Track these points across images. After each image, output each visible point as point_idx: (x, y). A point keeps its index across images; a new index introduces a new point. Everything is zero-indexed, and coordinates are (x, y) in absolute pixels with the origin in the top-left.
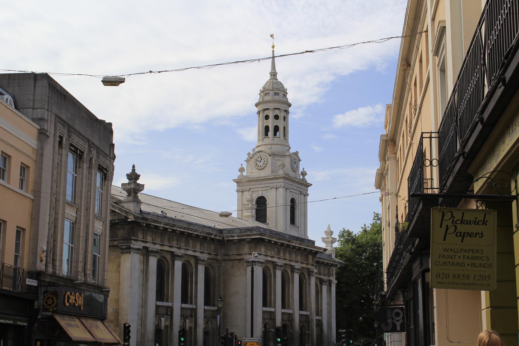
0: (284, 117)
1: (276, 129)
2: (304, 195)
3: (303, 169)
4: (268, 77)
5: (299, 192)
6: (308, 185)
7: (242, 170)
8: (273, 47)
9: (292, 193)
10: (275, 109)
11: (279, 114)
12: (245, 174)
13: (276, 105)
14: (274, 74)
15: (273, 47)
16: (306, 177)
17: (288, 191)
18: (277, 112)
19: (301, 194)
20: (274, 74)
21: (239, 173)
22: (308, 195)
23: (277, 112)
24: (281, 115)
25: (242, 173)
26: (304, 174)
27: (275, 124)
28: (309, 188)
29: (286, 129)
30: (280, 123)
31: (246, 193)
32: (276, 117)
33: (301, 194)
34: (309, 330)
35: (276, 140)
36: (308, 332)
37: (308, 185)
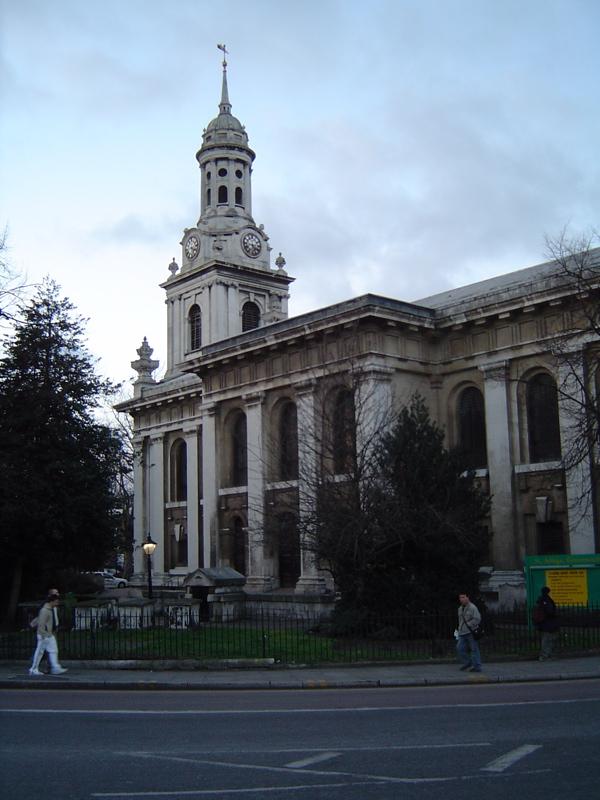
0: (239, 174)
1: (223, 191)
4: (215, 113)
6: (285, 280)
7: (173, 267)
8: (225, 65)
12: (178, 272)
14: (225, 107)
15: (225, 65)
16: (285, 268)
17: (231, 290)
20: (225, 107)
21: (170, 273)
23: (222, 165)
24: (232, 168)
25: (174, 273)
26: (281, 262)
28: (290, 285)
30: (231, 183)
31: (177, 302)
32: (223, 173)
33: (270, 295)
35: (223, 210)
37: (285, 280)
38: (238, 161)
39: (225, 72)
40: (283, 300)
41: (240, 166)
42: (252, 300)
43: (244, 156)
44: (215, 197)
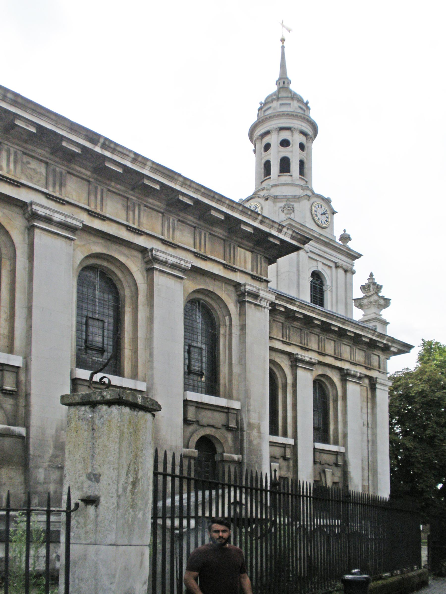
0: (302, 147)
2: (346, 271)
3: (345, 231)
5: (332, 265)
8: (283, 40)
9: (314, 263)
10: (282, 129)
11: (289, 138)
13: (282, 121)
14: (283, 82)
15: (283, 40)
18: (285, 135)
19: (337, 267)
22: (353, 273)
23: (285, 135)
26: (345, 238)
27: (283, 154)
28: (356, 262)
29: (306, 166)
32: (285, 143)
33: (337, 267)
34: (240, 451)
35: (285, 178)
36: (236, 457)
38: (303, 133)
39: (283, 47)
40: (349, 274)
41: (303, 139)
42: (320, 269)
43: (309, 130)
44: (275, 168)
